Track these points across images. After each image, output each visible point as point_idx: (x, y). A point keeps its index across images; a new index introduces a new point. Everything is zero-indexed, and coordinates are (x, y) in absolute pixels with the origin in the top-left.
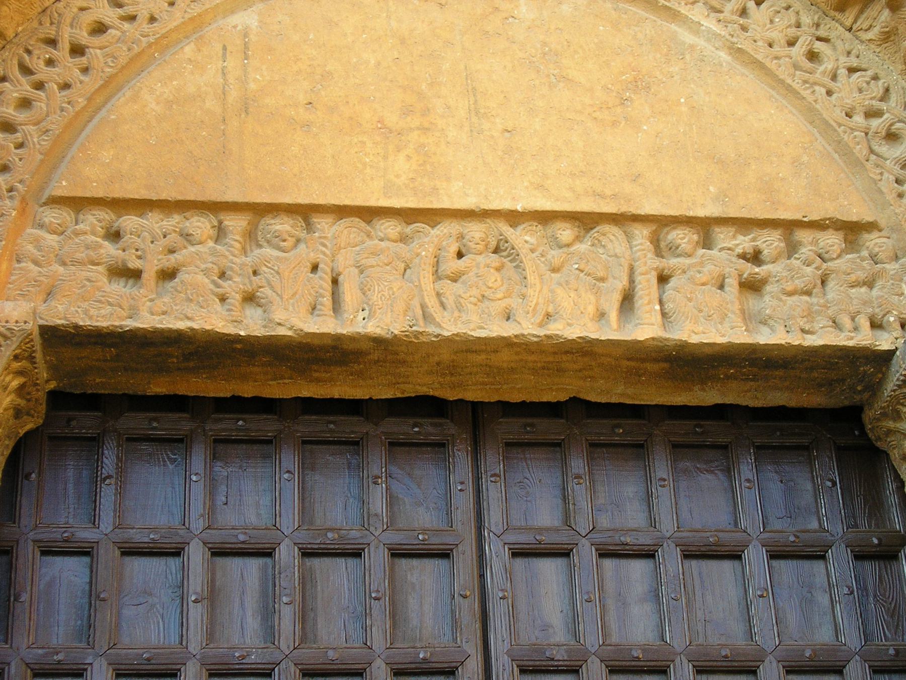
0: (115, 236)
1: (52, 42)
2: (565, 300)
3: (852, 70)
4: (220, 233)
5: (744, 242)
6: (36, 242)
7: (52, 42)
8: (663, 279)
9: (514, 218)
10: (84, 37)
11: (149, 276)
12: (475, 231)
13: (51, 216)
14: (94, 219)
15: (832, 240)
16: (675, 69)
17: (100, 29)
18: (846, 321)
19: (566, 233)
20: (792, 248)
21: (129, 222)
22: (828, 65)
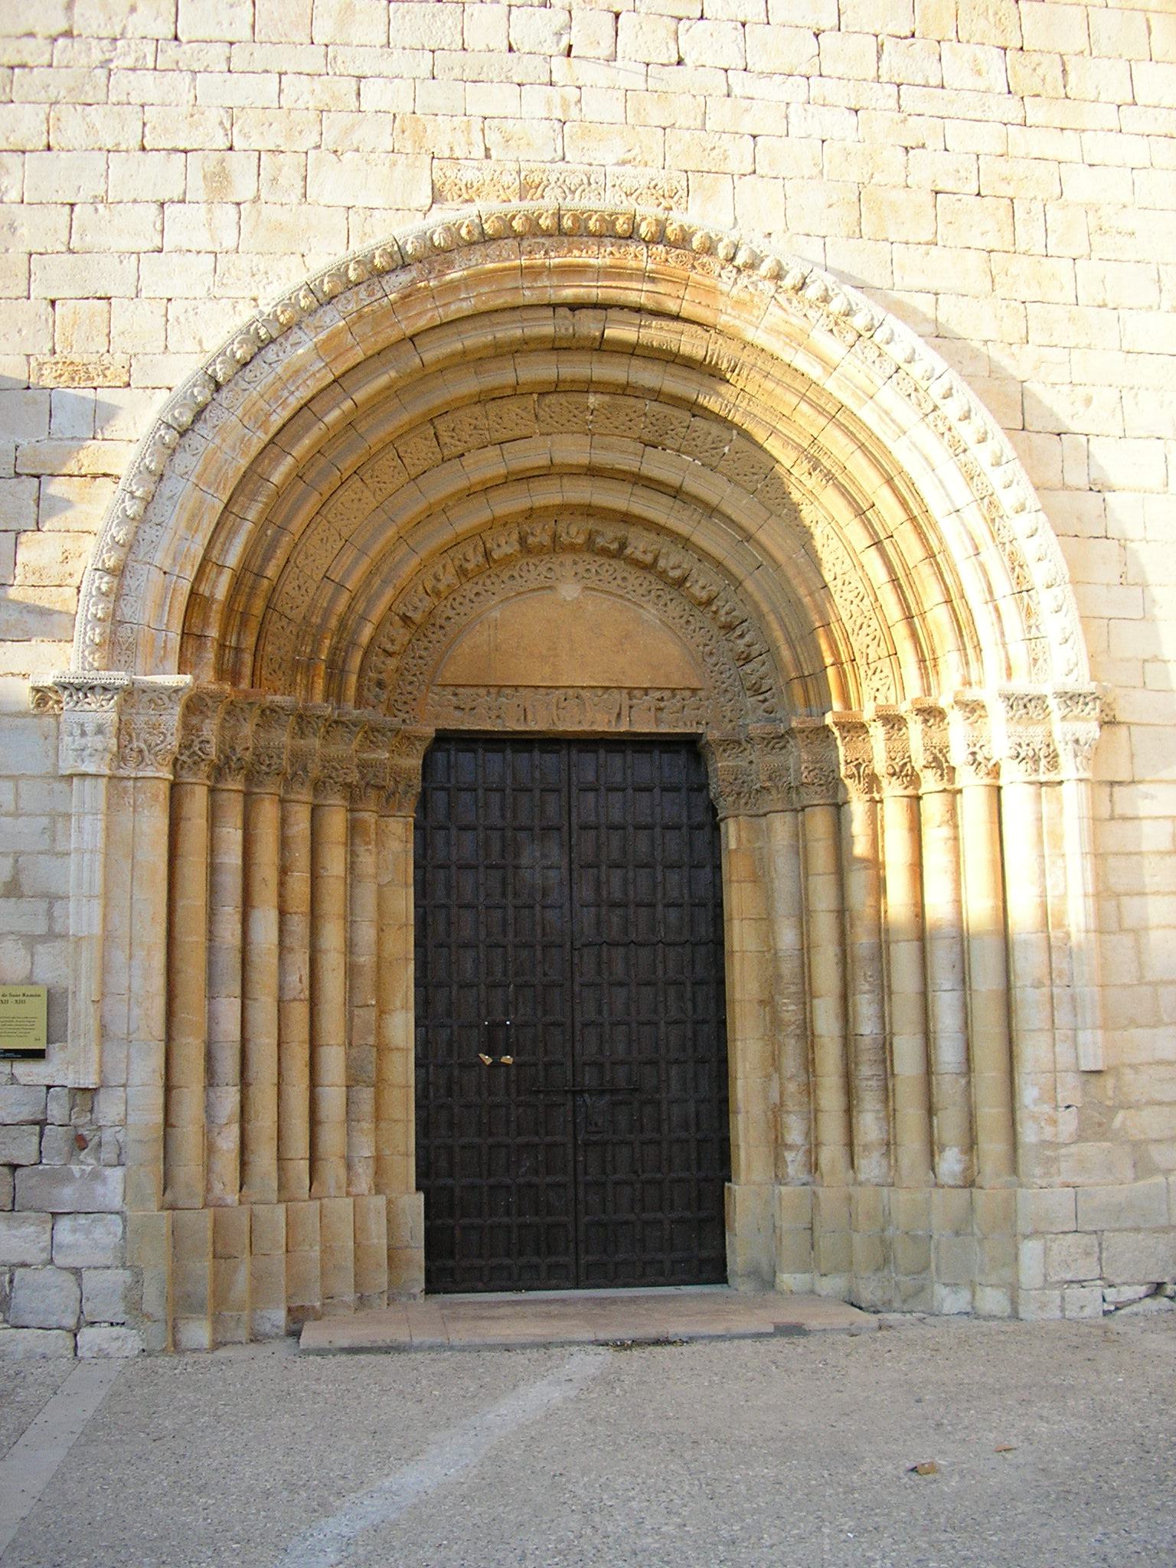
0: (455, 695)
1: (434, 625)
2: (599, 717)
3: (701, 628)
4: (489, 693)
5: (658, 695)
6: (432, 699)
7: (434, 625)
8: (631, 707)
9: (583, 688)
10: (443, 622)
11: (467, 710)
12: (570, 692)
13: (436, 689)
14: (449, 690)
15: (688, 693)
16: (640, 630)
17: (449, 618)
18: (689, 723)
19: (600, 692)
20: (674, 696)
21: (461, 690)
22: (692, 627)
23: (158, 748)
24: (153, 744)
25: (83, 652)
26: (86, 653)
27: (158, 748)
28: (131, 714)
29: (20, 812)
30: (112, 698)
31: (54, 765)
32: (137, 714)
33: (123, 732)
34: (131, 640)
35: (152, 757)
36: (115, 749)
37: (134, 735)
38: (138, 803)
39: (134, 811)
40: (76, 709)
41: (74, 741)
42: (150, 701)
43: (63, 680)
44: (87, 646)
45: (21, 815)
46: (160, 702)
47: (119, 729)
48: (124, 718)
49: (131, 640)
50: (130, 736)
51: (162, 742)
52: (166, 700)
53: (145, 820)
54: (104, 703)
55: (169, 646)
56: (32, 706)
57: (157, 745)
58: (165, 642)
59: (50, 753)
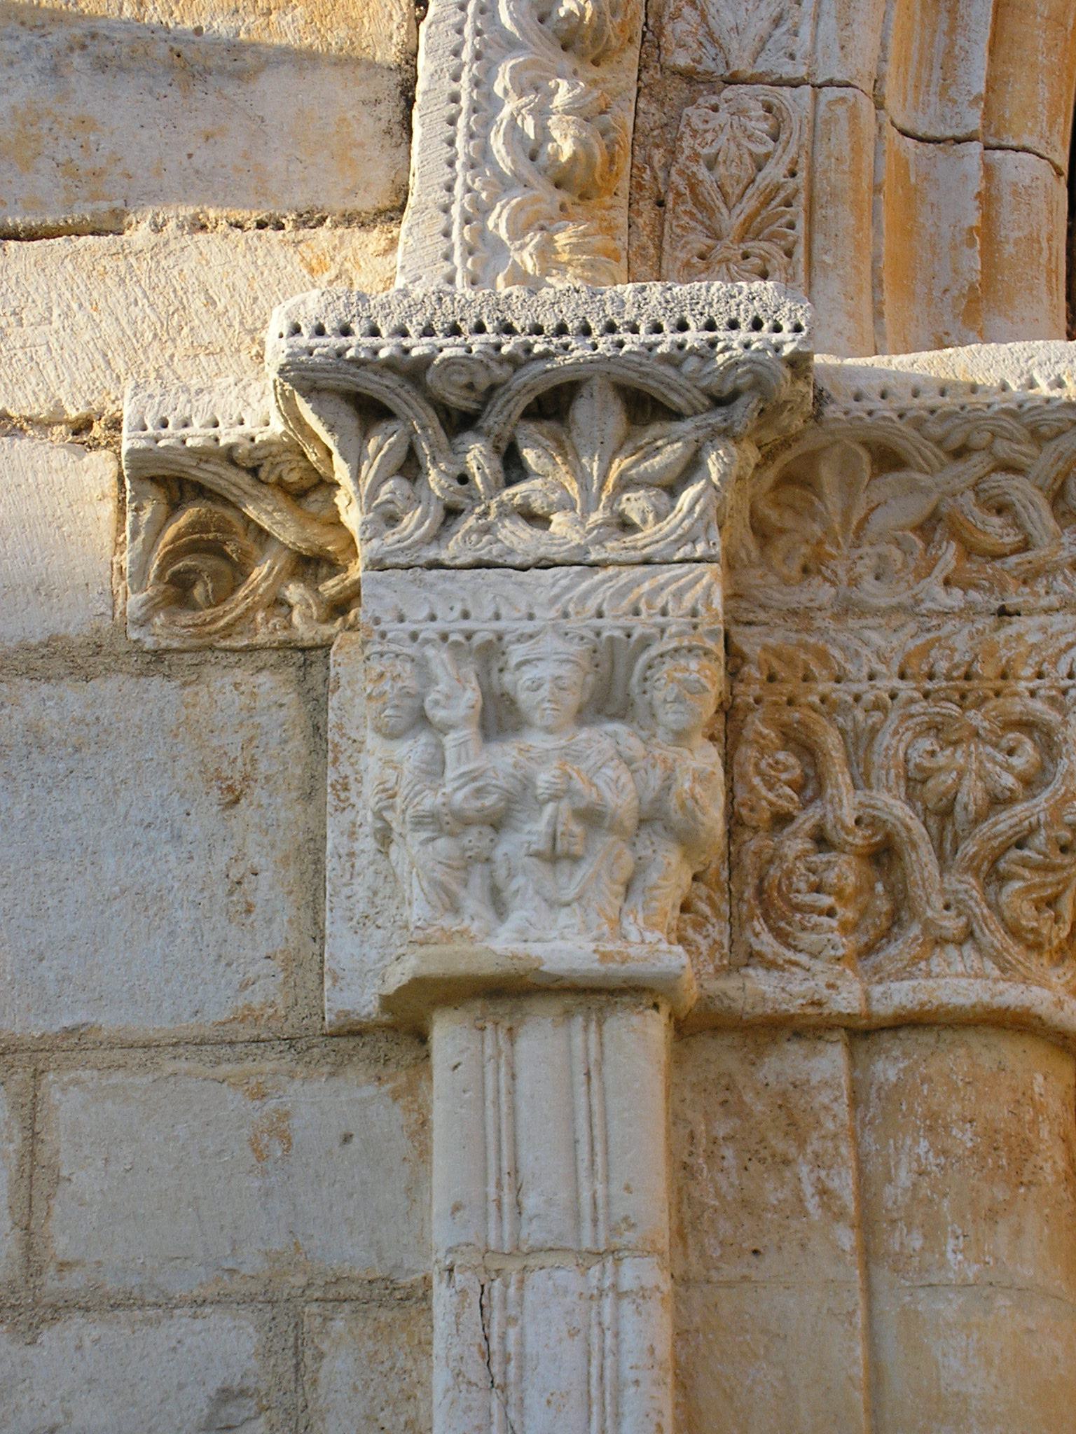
23: (1005, 822)
24: (971, 795)
25: (477, 214)
26: (498, 222)
27: (1005, 822)
28: (801, 616)
29: (51, 1283)
30: (692, 467)
31: (292, 963)
32: (847, 609)
33: (758, 725)
34: (774, 172)
35: (967, 885)
36: (714, 818)
37: (832, 741)
38: (893, 1194)
39: (868, 1254)
40: (453, 548)
41: (435, 768)
42: (928, 527)
43: (357, 345)
44: (502, 185)
45: (58, 1310)
46: (995, 530)
47: (729, 711)
48: (751, 642)
49: (774, 172)
50: (808, 750)
51: (1031, 783)
52: (1040, 517)
53: (949, 1308)
54: (635, 505)
55: (1012, 228)
56: (134, 602)
57: (998, 801)
58: (987, 200)
59: (263, 890)
